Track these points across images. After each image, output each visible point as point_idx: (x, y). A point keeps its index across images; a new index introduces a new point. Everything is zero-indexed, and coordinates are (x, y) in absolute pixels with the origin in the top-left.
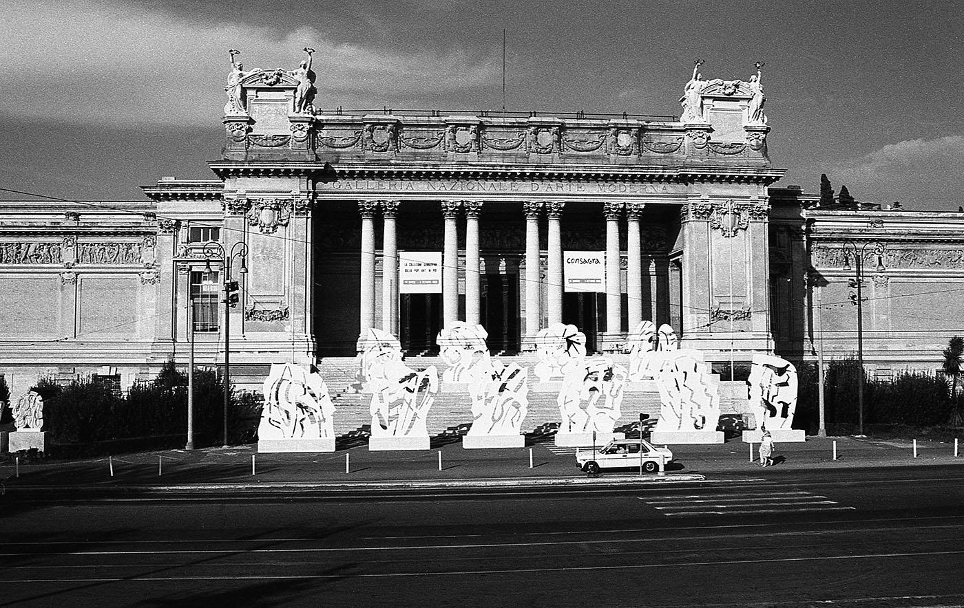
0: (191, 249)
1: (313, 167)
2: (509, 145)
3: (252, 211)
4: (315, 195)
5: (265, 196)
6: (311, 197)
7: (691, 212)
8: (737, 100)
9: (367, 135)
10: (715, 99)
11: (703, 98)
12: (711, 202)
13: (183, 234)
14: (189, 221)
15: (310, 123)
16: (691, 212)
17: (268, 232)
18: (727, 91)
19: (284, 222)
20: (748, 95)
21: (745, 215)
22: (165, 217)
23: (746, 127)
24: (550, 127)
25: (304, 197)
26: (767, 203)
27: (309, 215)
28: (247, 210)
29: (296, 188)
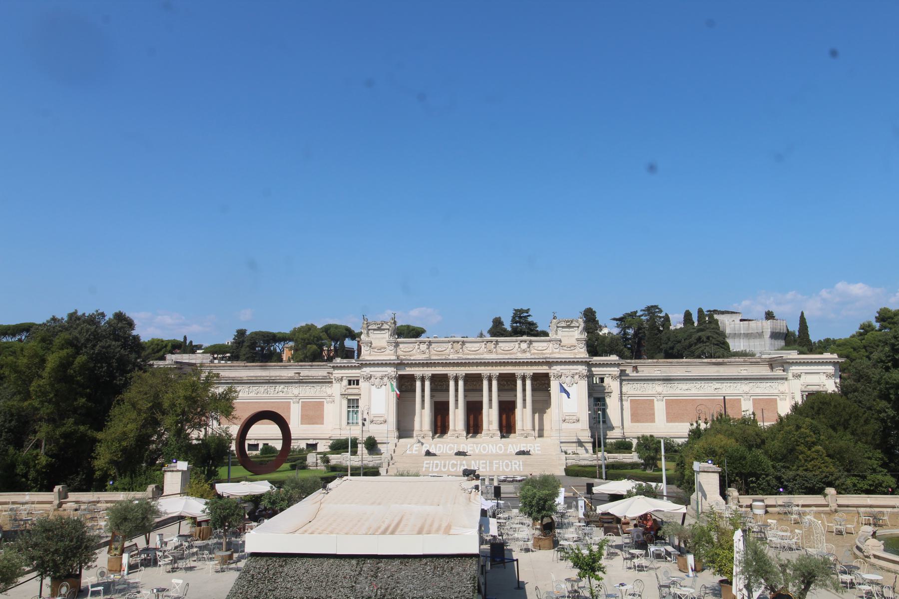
0: (347, 389)
1: (396, 362)
2: (476, 349)
3: (373, 379)
4: (397, 373)
5: (377, 373)
6: (395, 373)
7: (552, 377)
8: (573, 327)
9: (417, 347)
10: (563, 327)
11: (558, 327)
12: (561, 372)
13: (345, 382)
14: (347, 377)
15: (394, 343)
16: (552, 377)
17: (378, 388)
18: (568, 324)
19: (385, 384)
20: (577, 325)
21: (577, 377)
22: (337, 376)
23: (576, 339)
24: (492, 342)
25: (393, 373)
26: (586, 371)
27: (395, 381)
28: (370, 379)
29: (391, 371)
